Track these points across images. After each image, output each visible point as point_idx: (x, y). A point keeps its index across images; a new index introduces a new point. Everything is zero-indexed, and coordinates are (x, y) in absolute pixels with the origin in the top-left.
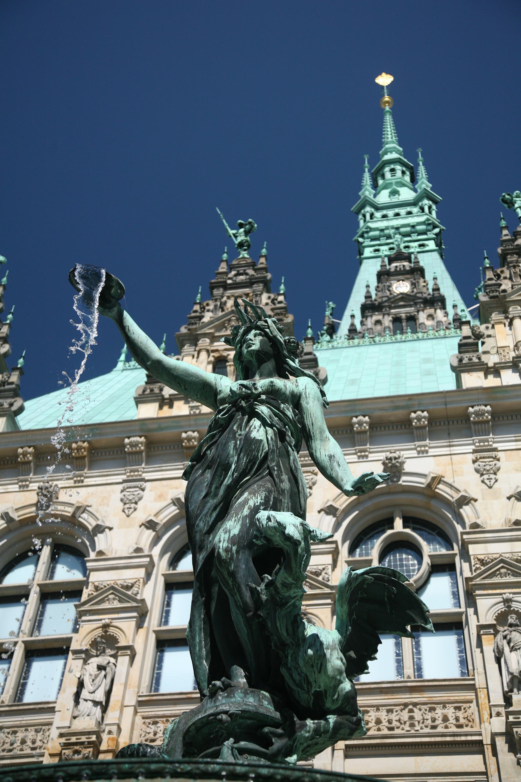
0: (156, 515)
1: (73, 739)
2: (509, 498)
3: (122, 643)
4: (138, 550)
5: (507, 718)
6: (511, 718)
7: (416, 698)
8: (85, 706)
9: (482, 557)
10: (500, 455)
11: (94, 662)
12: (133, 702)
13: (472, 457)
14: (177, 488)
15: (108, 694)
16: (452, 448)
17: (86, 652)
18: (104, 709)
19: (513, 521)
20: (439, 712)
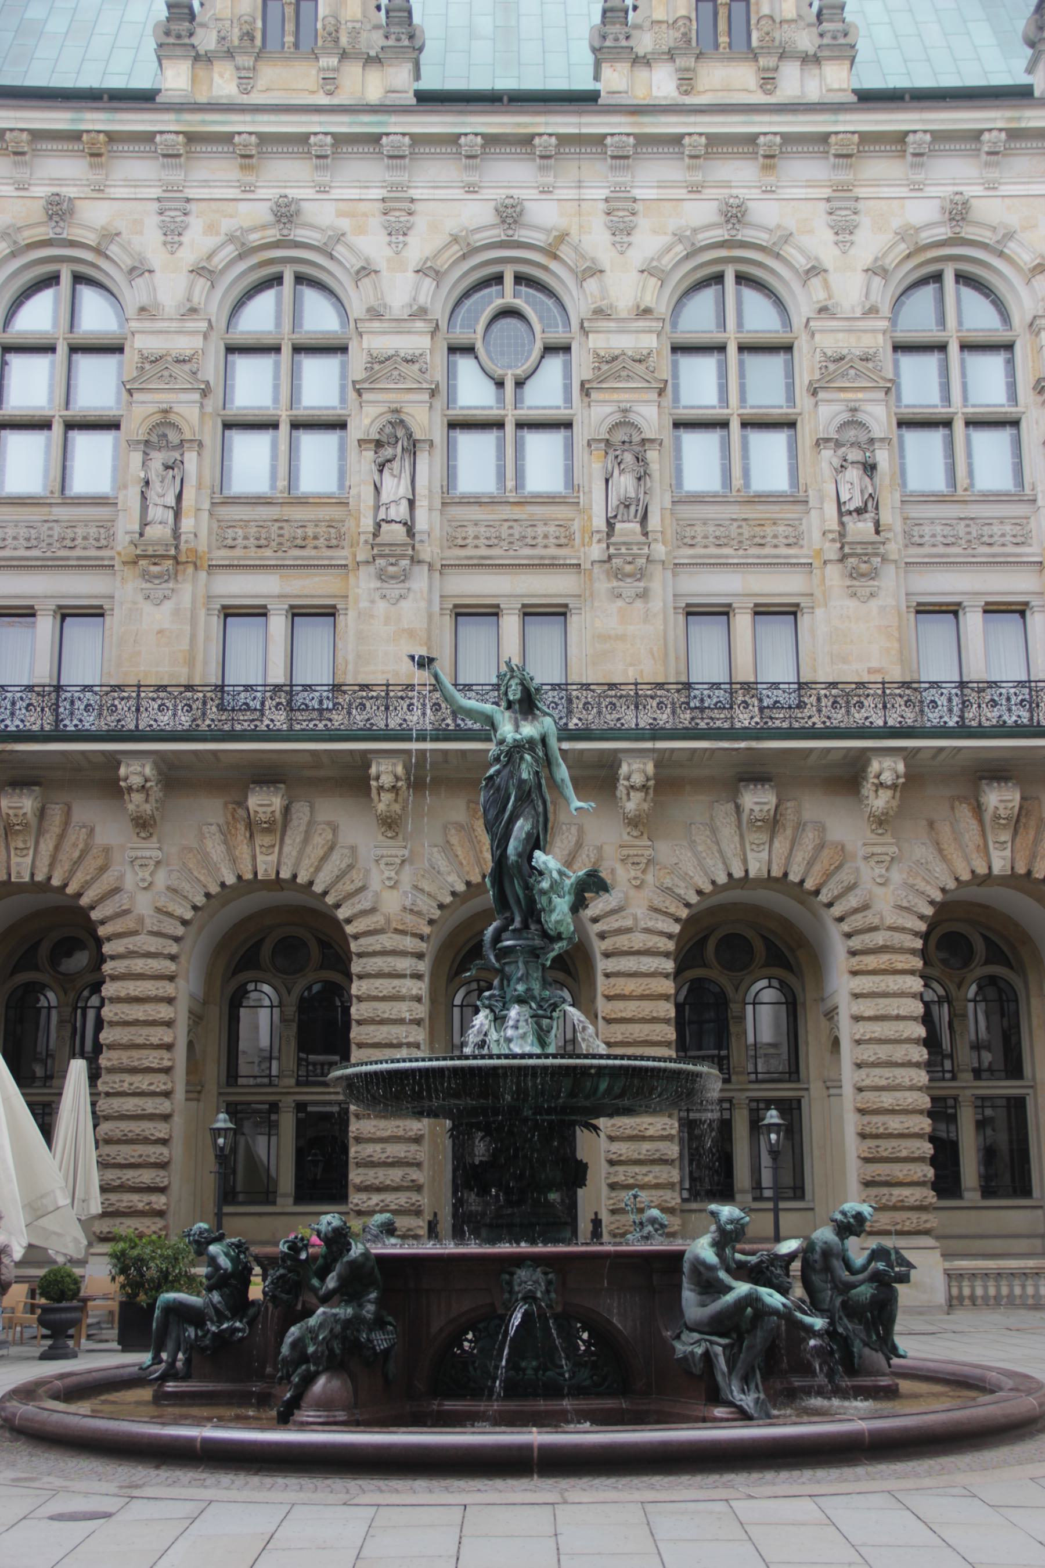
0: (210, 257)
1: (150, 553)
2: (642, 271)
3: (188, 436)
4: (193, 310)
5: (608, 548)
6: (612, 551)
7: (517, 513)
8: (155, 513)
9: (602, 354)
10: (639, 207)
11: (158, 458)
12: (206, 505)
13: (602, 206)
14: (231, 216)
15: (179, 497)
16: (583, 191)
17: (147, 442)
18: (177, 514)
19: (642, 307)
20: (541, 530)
